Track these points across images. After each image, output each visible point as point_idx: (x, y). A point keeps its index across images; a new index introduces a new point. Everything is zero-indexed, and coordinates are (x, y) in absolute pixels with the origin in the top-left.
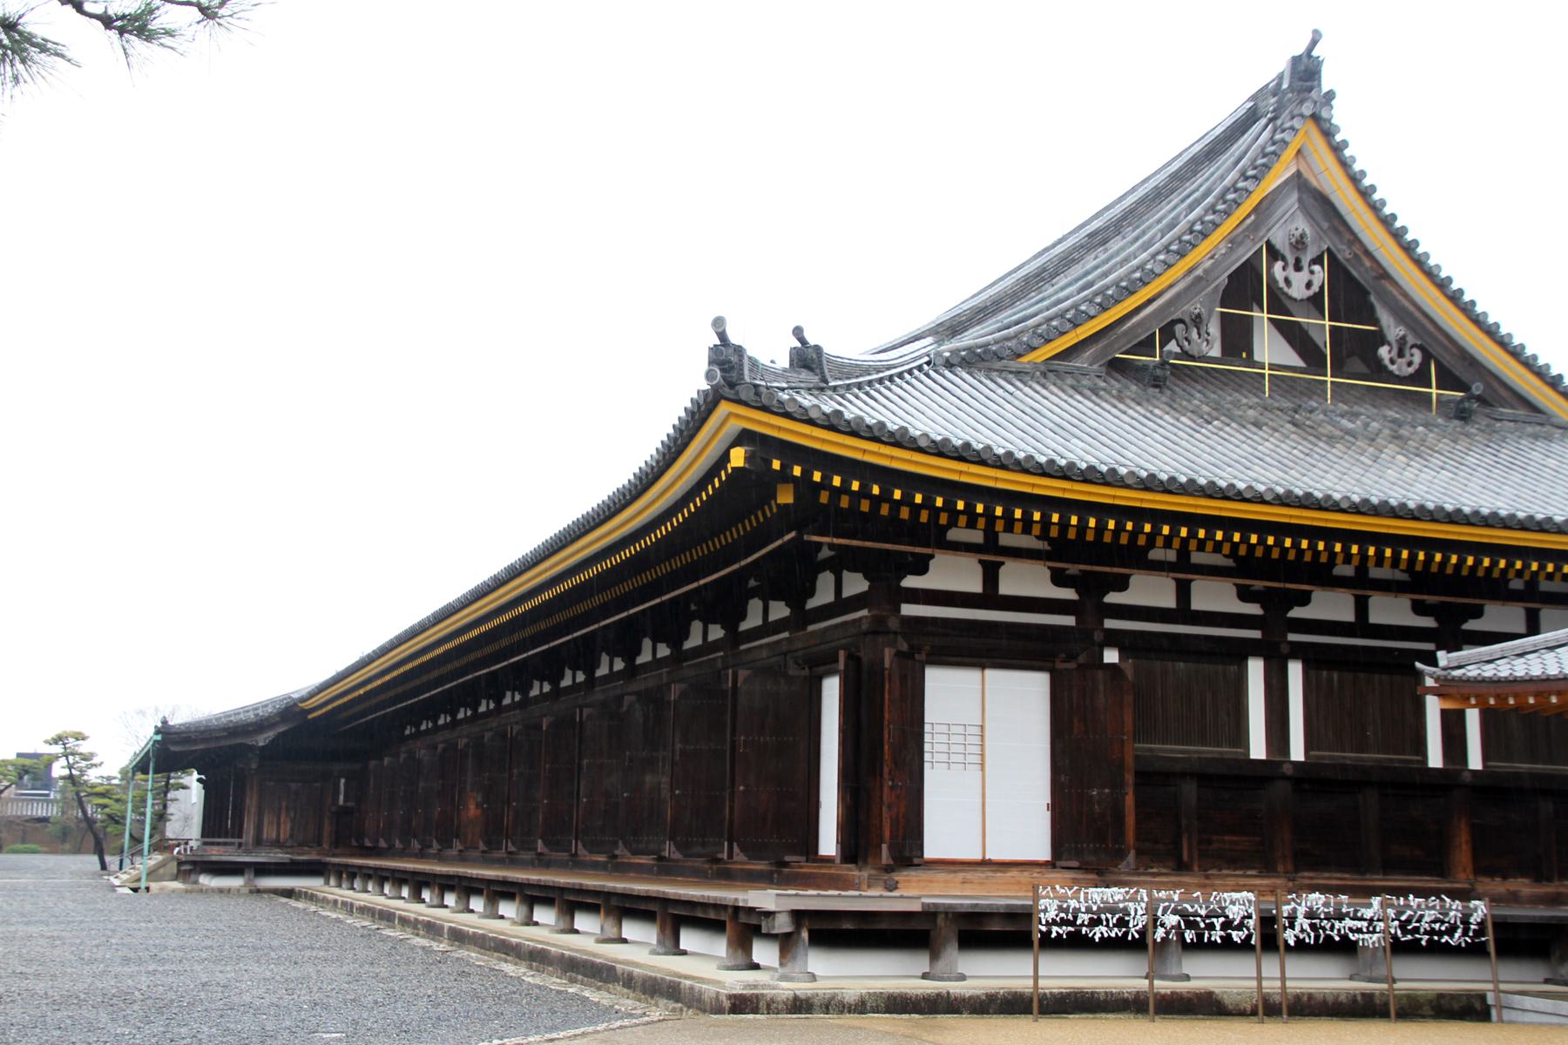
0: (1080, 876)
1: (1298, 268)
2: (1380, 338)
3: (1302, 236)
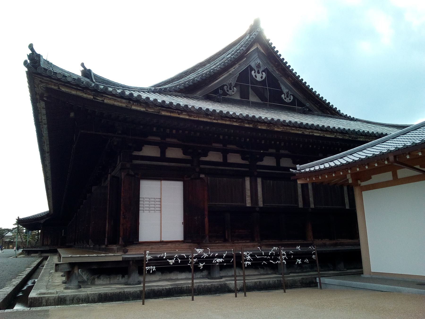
0: (192, 244)
1: (259, 73)
2: (282, 93)
3: (259, 64)
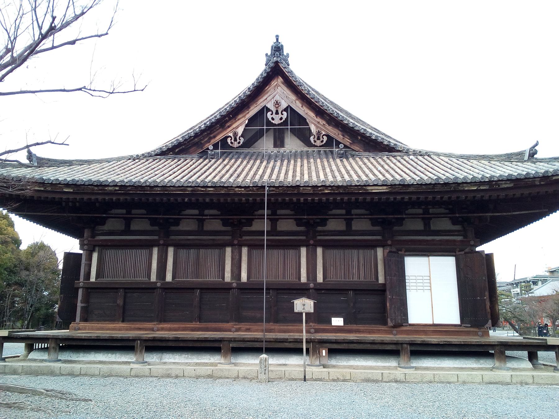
2: (310, 133)
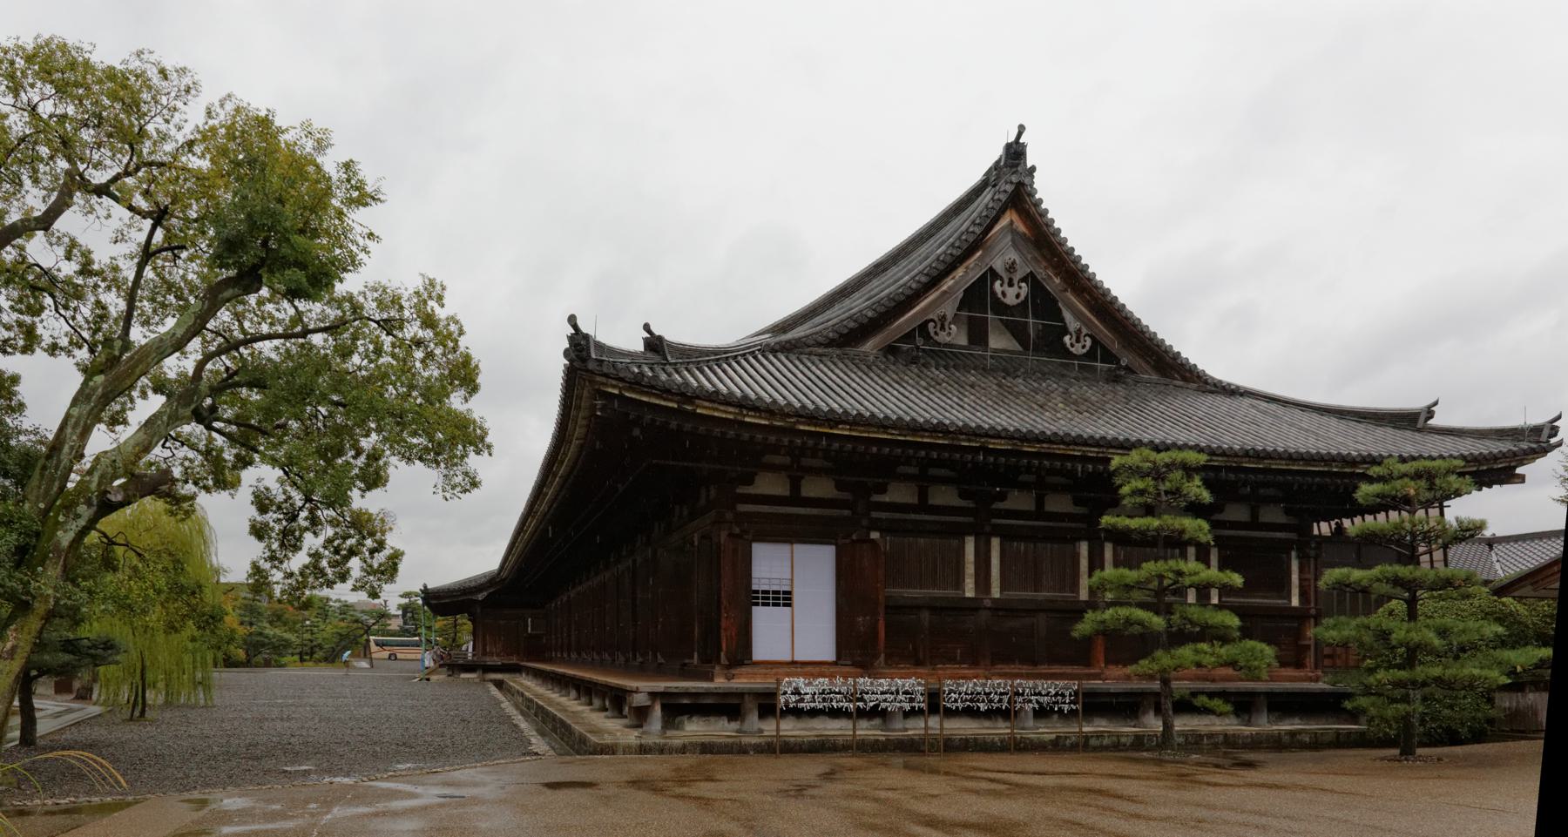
1: (1011, 284)
2: (1065, 331)
3: (1014, 263)
